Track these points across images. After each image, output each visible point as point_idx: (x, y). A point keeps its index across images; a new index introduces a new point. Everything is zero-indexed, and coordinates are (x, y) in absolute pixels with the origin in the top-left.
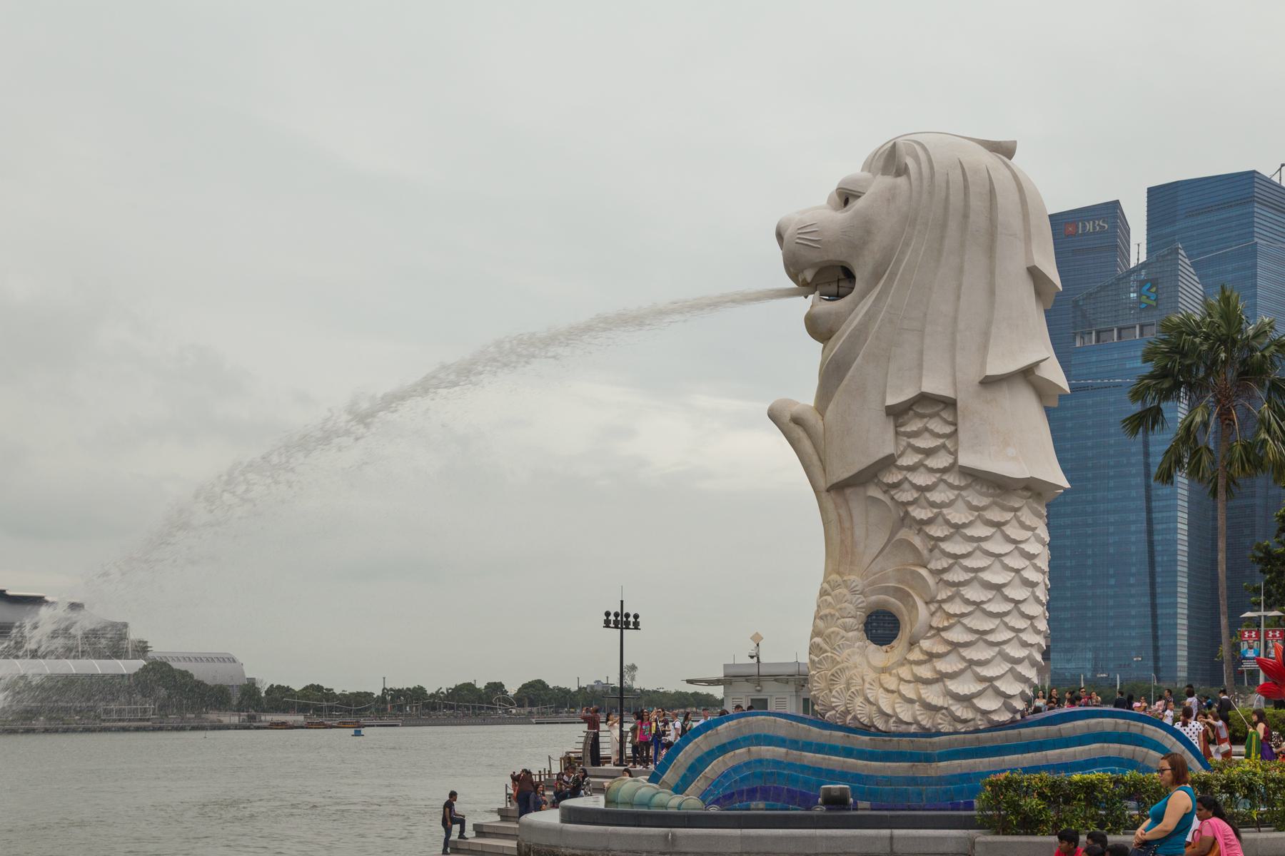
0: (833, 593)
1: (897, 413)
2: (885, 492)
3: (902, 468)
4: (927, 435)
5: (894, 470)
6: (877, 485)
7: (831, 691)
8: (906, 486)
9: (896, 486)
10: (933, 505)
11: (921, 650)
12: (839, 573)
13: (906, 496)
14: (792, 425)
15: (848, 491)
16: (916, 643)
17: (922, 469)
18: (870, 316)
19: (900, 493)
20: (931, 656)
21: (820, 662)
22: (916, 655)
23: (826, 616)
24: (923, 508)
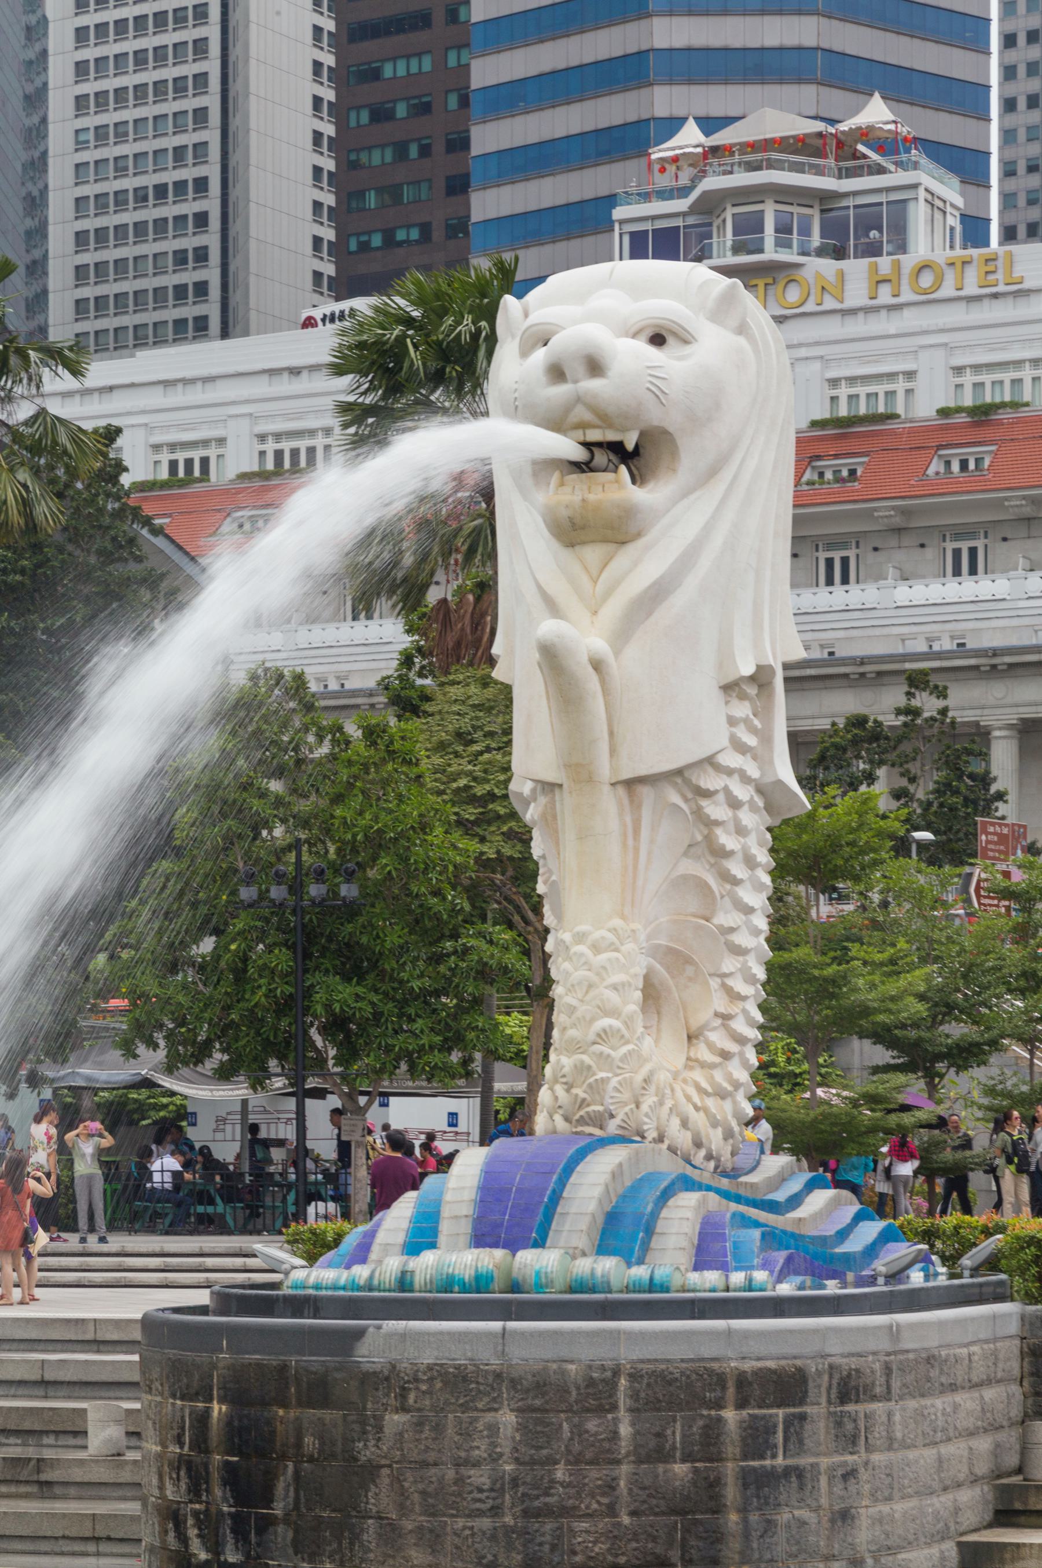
0: (623, 948)
1: (731, 688)
2: (686, 800)
3: (719, 768)
4: (742, 726)
5: (710, 770)
6: (675, 785)
7: (638, 1107)
8: (721, 797)
9: (707, 794)
10: (741, 831)
11: (711, 1046)
12: (623, 917)
13: (717, 810)
14: (590, 669)
15: (646, 792)
16: (697, 1037)
17: (736, 776)
18: (708, 529)
19: (712, 807)
20: (726, 1055)
21: (624, 1058)
22: (703, 1053)
23: (623, 985)
24: (728, 833)
